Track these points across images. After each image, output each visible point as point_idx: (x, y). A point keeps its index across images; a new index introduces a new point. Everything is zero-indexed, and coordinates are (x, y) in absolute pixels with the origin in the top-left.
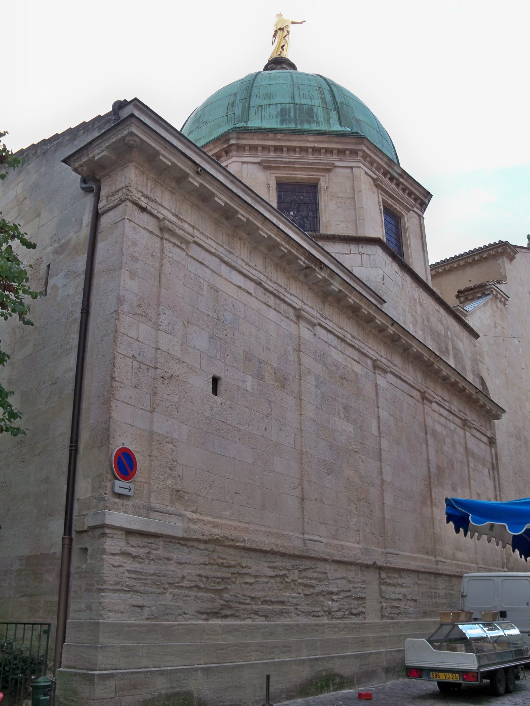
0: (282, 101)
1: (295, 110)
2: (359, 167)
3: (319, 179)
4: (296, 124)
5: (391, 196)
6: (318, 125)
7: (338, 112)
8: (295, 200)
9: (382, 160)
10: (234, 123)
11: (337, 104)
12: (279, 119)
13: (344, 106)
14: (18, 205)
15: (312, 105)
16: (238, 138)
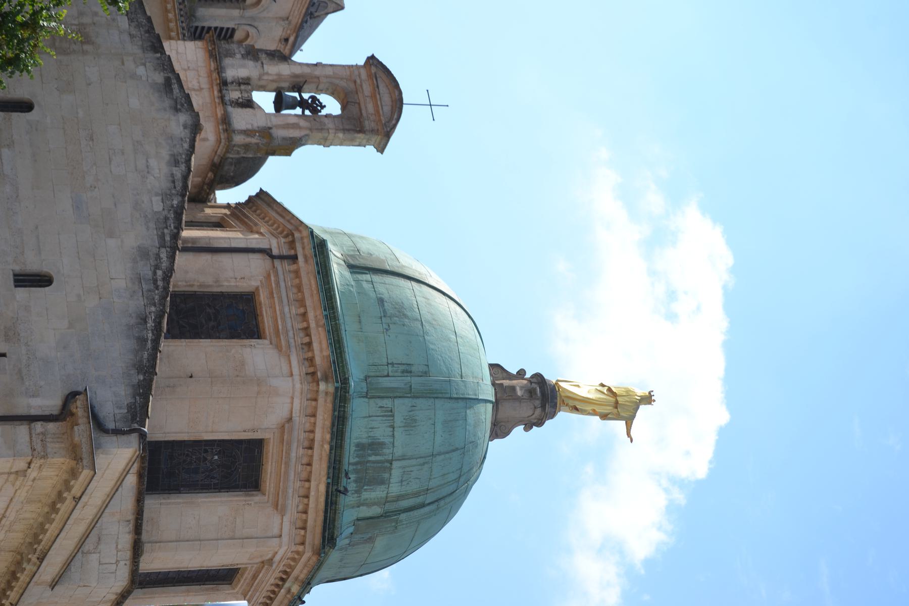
0: (396, 444)
2: (280, 546)
3: (264, 494)
4: (356, 464)
5: (255, 577)
6: (353, 492)
7: (382, 516)
8: (236, 462)
9: (301, 572)
10: (369, 377)
11: (396, 515)
12: (364, 441)
13: (393, 524)
14: (98, 286)
15: (389, 483)
16: (327, 393)
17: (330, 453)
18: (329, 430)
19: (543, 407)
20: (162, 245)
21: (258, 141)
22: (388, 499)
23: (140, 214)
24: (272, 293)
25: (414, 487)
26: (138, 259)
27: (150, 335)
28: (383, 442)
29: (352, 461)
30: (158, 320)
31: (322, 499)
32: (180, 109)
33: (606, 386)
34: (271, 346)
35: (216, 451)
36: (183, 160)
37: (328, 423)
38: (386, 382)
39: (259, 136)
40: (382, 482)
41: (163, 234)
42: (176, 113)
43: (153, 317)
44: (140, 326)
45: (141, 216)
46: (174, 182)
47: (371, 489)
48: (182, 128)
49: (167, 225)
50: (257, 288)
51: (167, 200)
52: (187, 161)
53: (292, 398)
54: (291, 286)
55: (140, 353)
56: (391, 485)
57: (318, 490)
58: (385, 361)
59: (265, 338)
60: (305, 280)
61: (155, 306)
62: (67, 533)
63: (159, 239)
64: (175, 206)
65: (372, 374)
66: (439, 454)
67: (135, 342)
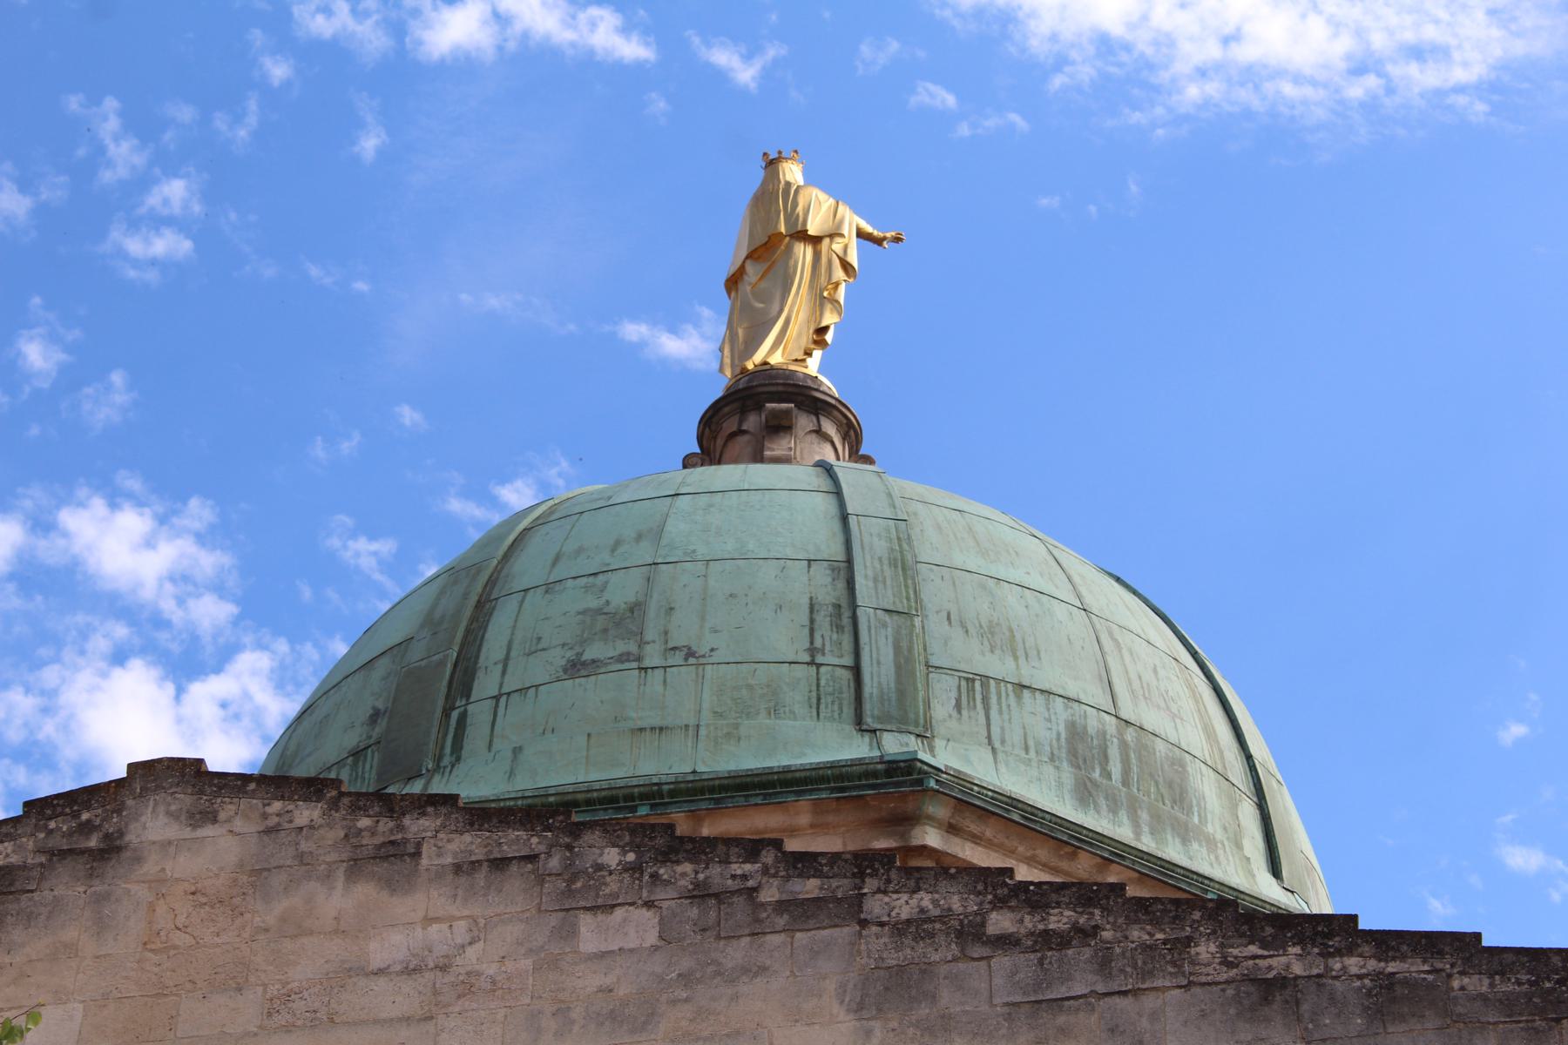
1: (1124, 745)
16: (952, 829)
20: (852, 910)
23: (674, 1002)
26: (924, 1011)
27: (1353, 964)
28: (1066, 727)
30: (1269, 930)
32: (107, 836)
33: (742, 268)
36: (386, 825)
41: (782, 906)
42: (126, 854)
43: (1253, 949)
44: (1305, 1007)
45: (687, 1000)
46: (499, 864)
47: (1199, 805)
48: (208, 831)
49: (739, 892)
51: (598, 889)
52: (392, 810)
55: (1460, 1009)
61: (1188, 941)
63: (812, 923)
64: (631, 857)
65: (848, 711)
67: (1403, 1027)
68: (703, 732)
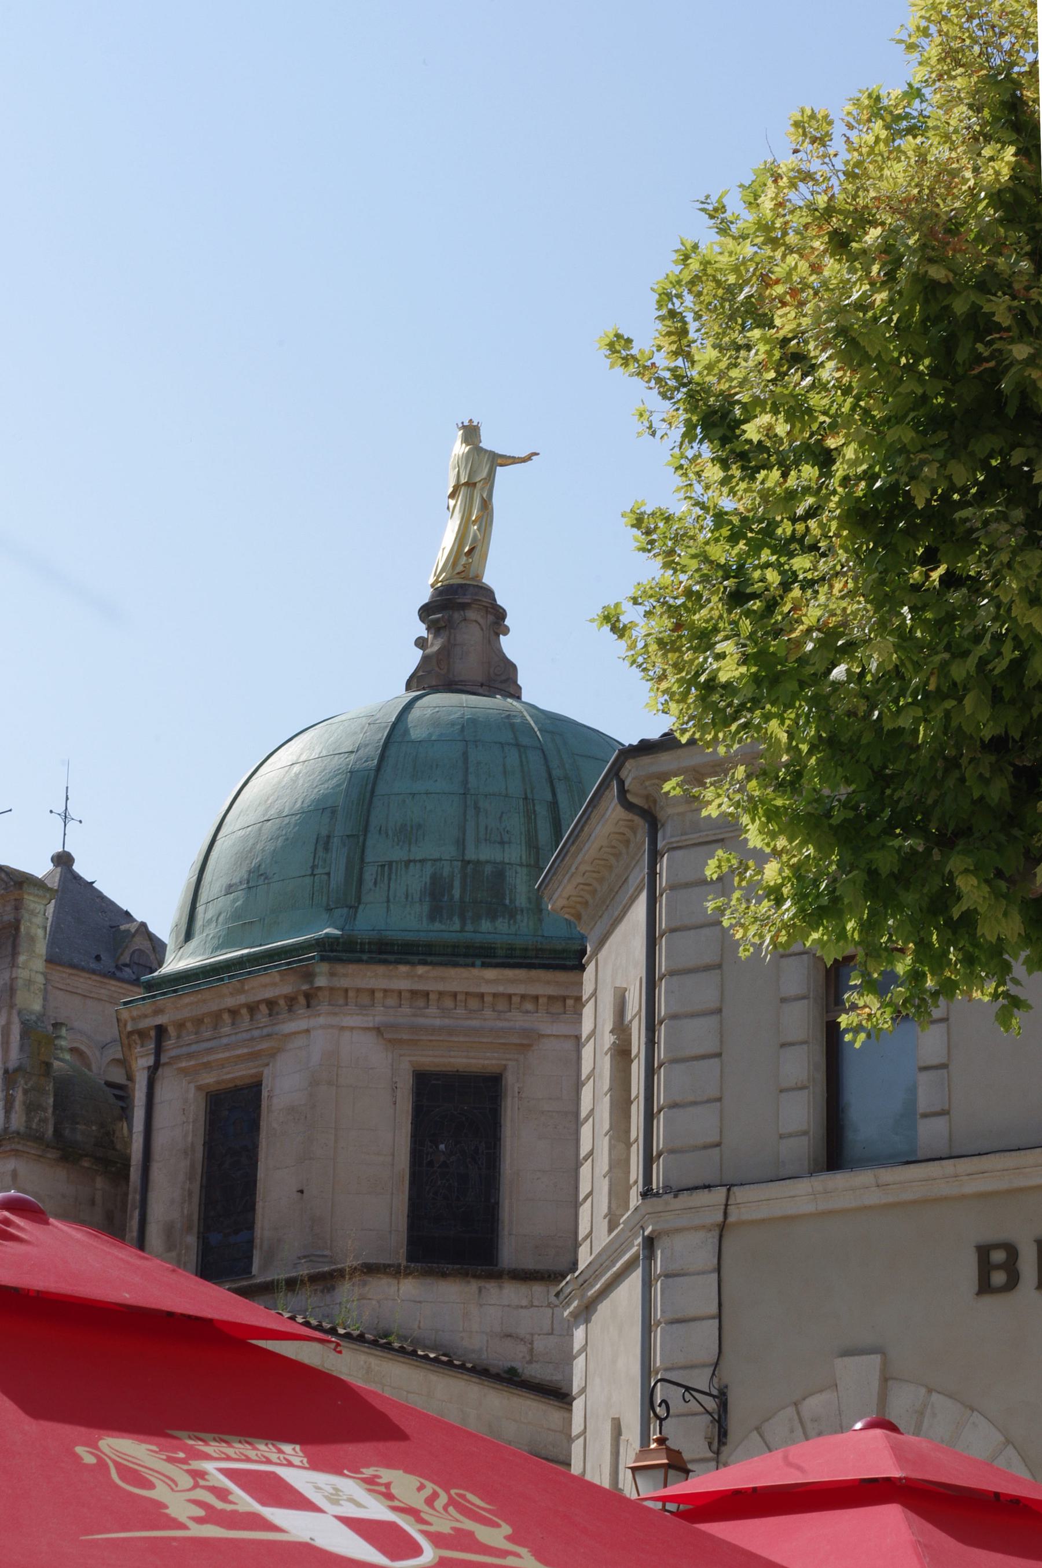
0: (436, 856)
3: (505, 1066)
6: (512, 922)
10: (328, 905)
12: (426, 908)
15: (503, 863)
16: (332, 974)
17: (431, 964)
18: (391, 967)
19: (464, 606)
21: (20, 1089)
22: (532, 863)
24: (207, 1065)
25: (515, 823)
28: (431, 878)
29: (457, 926)
31: (510, 973)
34: (271, 1065)
35: (431, 1147)
37: (381, 969)
38: (338, 876)
39: (13, 1089)
40: (500, 873)
50: (199, 1088)
53: (342, 1028)
54: (196, 1034)
56: (507, 861)
57: (496, 981)
58: (308, 880)
59: (262, 1074)
60: (186, 1013)
62: (408, 1392)
65: (325, 899)
66: (465, 783)
68: (266, 921)
